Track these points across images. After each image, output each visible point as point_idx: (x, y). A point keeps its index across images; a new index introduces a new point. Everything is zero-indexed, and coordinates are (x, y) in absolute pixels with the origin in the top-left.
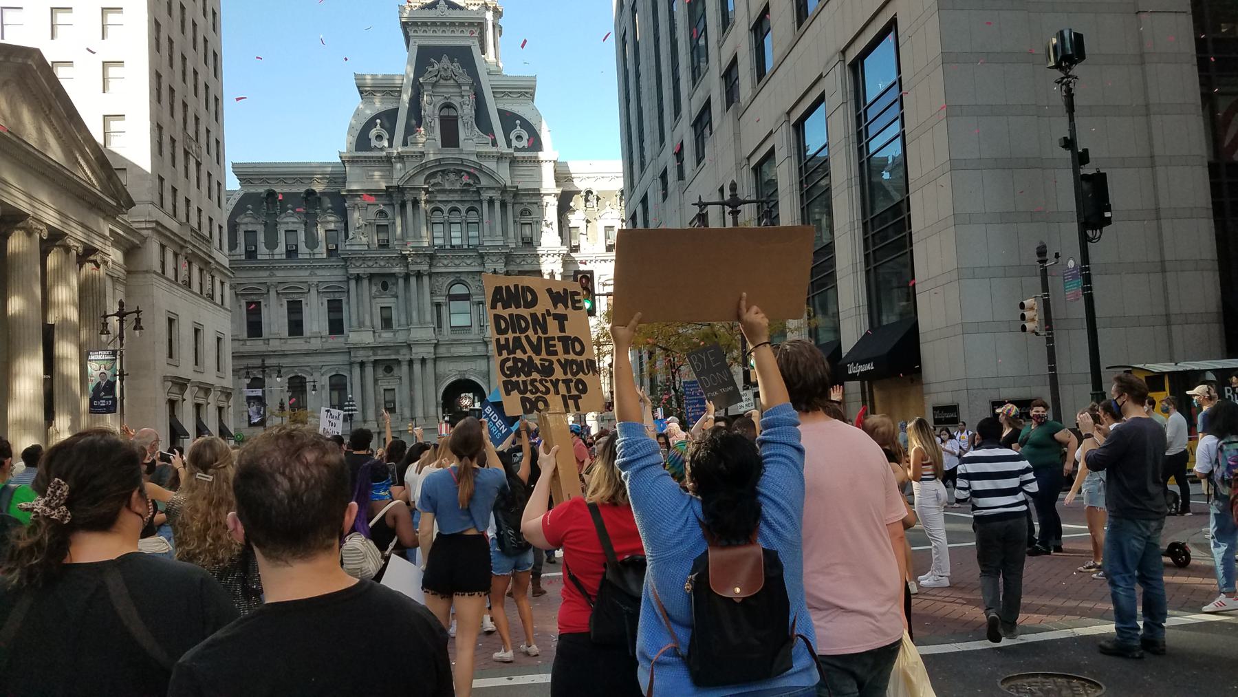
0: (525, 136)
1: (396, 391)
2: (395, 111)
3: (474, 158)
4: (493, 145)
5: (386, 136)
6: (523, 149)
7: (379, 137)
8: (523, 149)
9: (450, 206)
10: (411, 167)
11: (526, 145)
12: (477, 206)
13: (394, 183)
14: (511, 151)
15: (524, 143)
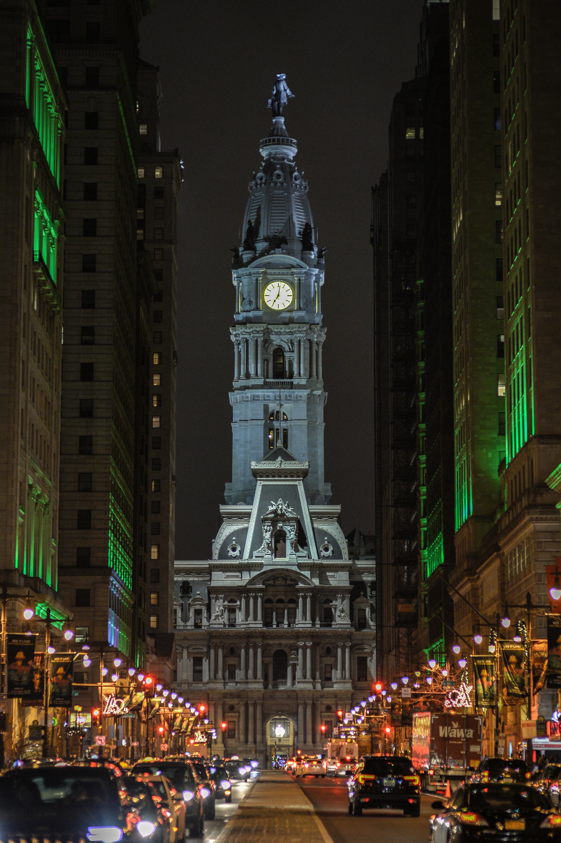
0: (331, 548)
1: (236, 723)
2: (246, 529)
3: (295, 568)
4: (309, 558)
5: (239, 549)
6: (328, 558)
7: (234, 550)
8: (328, 558)
9: (277, 598)
10: (254, 574)
11: (331, 554)
12: (295, 598)
13: (243, 583)
14: (319, 562)
15: (329, 553)
